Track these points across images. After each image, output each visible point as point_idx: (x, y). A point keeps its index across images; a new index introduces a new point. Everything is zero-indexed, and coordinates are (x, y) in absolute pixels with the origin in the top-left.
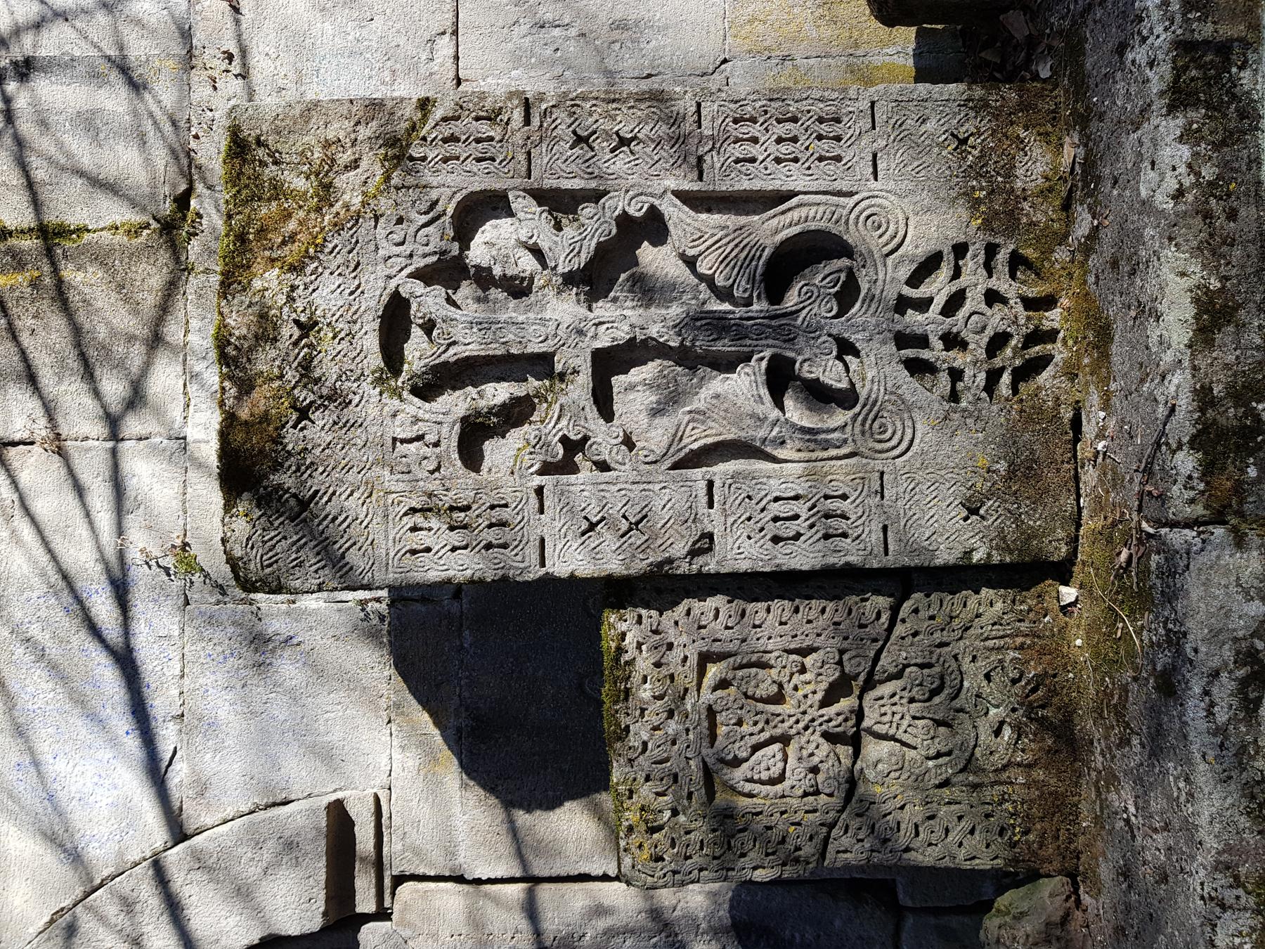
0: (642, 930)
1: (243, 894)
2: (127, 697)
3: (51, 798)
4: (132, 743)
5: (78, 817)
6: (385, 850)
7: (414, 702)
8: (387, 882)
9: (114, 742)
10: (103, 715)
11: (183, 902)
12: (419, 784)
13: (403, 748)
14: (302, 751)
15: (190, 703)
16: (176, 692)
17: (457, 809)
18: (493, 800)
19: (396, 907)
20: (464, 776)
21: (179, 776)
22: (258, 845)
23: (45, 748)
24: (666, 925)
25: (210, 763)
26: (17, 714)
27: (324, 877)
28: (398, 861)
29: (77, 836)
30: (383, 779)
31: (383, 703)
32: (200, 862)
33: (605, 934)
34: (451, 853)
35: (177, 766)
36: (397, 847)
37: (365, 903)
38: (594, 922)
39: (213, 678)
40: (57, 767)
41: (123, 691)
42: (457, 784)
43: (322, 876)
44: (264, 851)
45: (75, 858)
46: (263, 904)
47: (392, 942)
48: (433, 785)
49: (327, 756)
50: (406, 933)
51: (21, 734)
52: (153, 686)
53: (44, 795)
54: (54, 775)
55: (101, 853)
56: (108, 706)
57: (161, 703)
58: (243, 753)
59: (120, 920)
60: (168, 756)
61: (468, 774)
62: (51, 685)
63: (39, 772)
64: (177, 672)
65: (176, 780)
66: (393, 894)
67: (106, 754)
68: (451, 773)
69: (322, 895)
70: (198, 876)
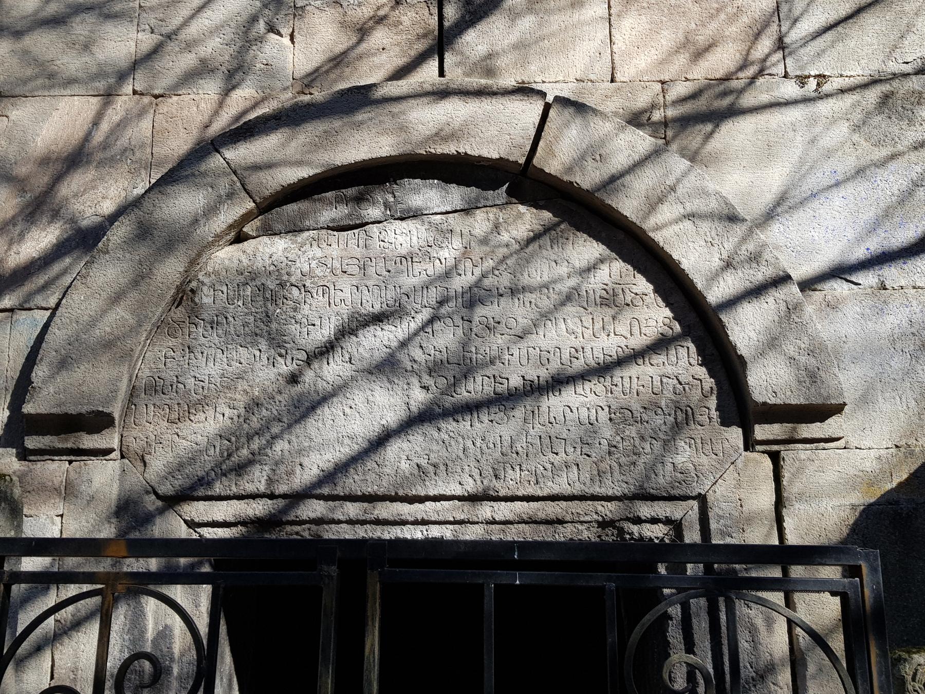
0: (758, 657)
1: (772, 343)
2: (895, 248)
3: (814, 195)
4: (860, 253)
5: (801, 215)
6: (800, 446)
7: (914, 467)
8: (775, 448)
9: (859, 240)
10: (879, 231)
11: (762, 298)
12: (852, 472)
13: (879, 458)
14: (868, 379)
15: (897, 294)
16: (903, 283)
17: (836, 502)
18: (845, 531)
19: (755, 455)
20: (862, 507)
21: (839, 288)
22: (811, 352)
23: (849, 190)
24: (762, 677)
25: (852, 310)
26: (872, 169)
27: (793, 403)
28: (792, 456)
29: (787, 216)
30: (854, 442)
31: (912, 441)
32: (792, 309)
33: (752, 625)
34: (800, 497)
35: (846, 285)
36: (803, 455)
37: (761, 432)
38: (760, 615)
39: (918, 311)
40: (837, 199)
41: (899, 245)
42: (855, 501)
43: (794, 401)
44: (807, 357)
45: (769, 216)
46: (767, 357)
47: (732, 452)
48: (852, 484)
49: (865, 400)
50: (740, 463)
51: (858, 172)
52: (905, 267)
53: (815, 191)
54: (830, 197)
55: (776, 234)
56: (887, 235)
57: (893, 274)
58: (863, 335)
59: (743, 252)
60: (854, 279)
61: (864, 511)
62: (896, 192)
63: (830, 187)
64: (918, 284)
65: (835, 286)
66: (763, 452)
67: (850, 234)
68: (860, 498)
69: (779, 402)
70: (783, 307)
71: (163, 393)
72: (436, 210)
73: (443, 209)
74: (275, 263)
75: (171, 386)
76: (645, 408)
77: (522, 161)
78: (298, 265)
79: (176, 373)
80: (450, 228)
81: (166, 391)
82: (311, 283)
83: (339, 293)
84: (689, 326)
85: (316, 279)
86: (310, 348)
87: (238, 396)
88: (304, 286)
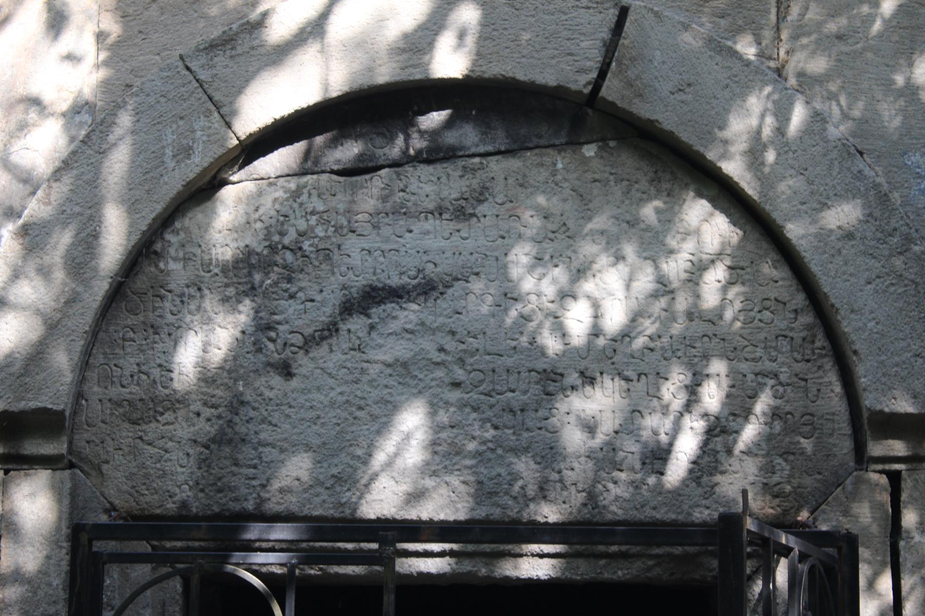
71: (123, 386)
72: (473, 150)
73: (482, 149)
74: (263, 218)
75: (132, 376)
76: (734, 415)
77: (587, 90)
78: (293, 221)
79: (138, 360)
80: (492, 175)
81: (125, 383)
82: (311, 245)
83: (346, 260)
84: (796, 311)
85: (316, 240)
86: (308, 331)
87: (219, 392)
88: (300, 248)
